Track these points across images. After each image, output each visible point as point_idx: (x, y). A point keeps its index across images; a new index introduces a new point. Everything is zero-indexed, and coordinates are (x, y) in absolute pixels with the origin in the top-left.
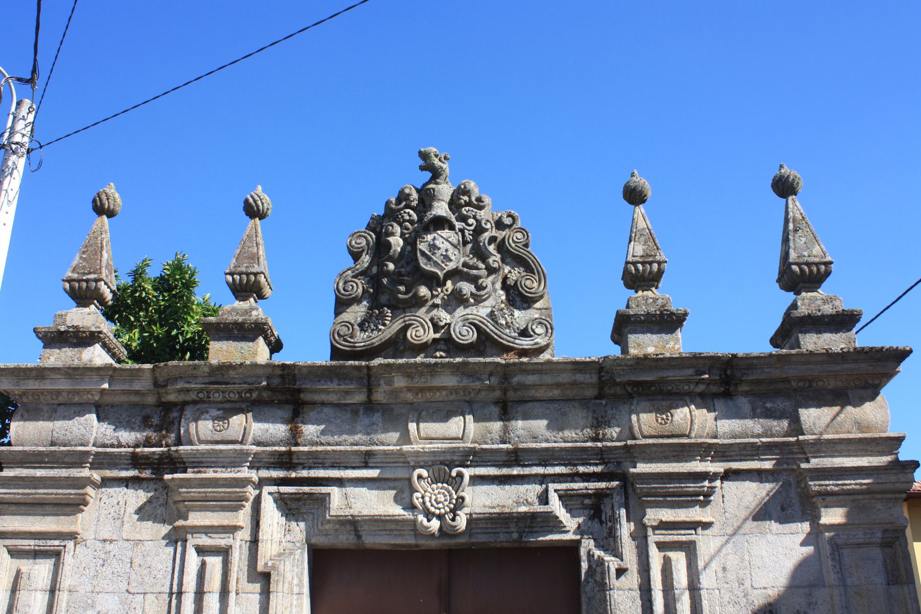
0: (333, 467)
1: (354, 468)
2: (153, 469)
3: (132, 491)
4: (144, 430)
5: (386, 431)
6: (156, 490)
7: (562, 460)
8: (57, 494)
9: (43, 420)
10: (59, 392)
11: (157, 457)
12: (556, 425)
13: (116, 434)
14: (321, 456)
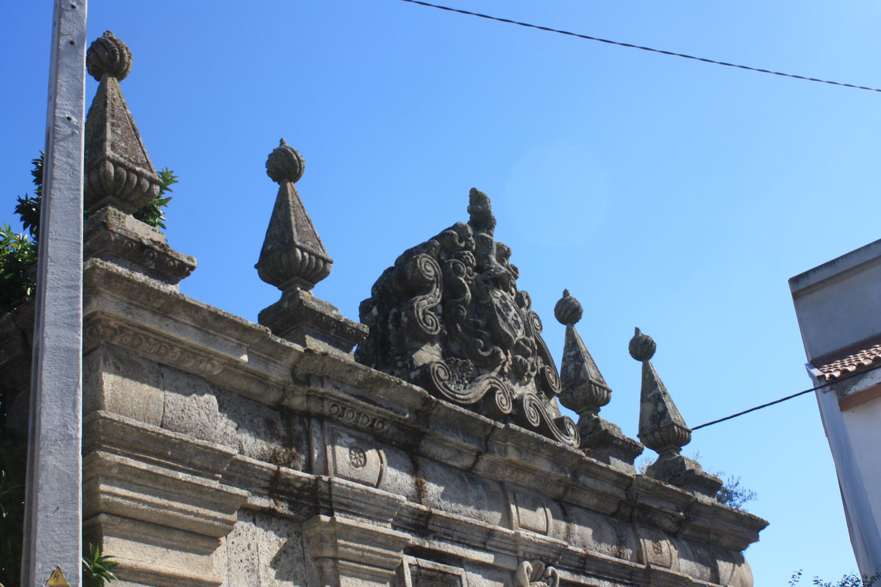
0: (460, 542)
1: (475, 548)
2: (290, 502)
3: (262, 530)
4: (271, 441)
5: (491, 509)
6: (288, 536)
7: (611, 575)
8: (197, 515)
9: (149, 384)
10: (172, 343)
11: (299, 485)
12: (598, 537)
13: (239, 436)
14: (453, 526)
